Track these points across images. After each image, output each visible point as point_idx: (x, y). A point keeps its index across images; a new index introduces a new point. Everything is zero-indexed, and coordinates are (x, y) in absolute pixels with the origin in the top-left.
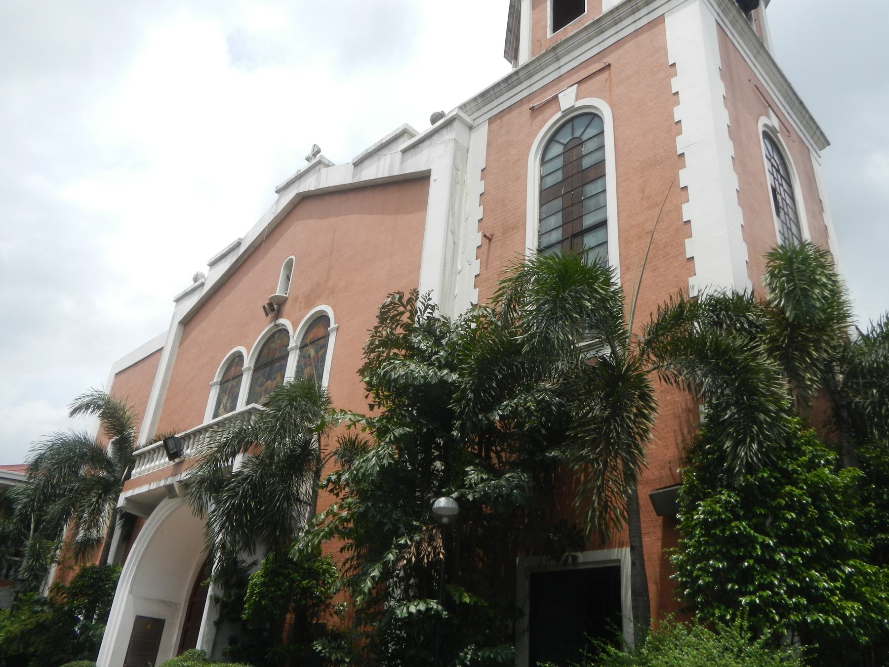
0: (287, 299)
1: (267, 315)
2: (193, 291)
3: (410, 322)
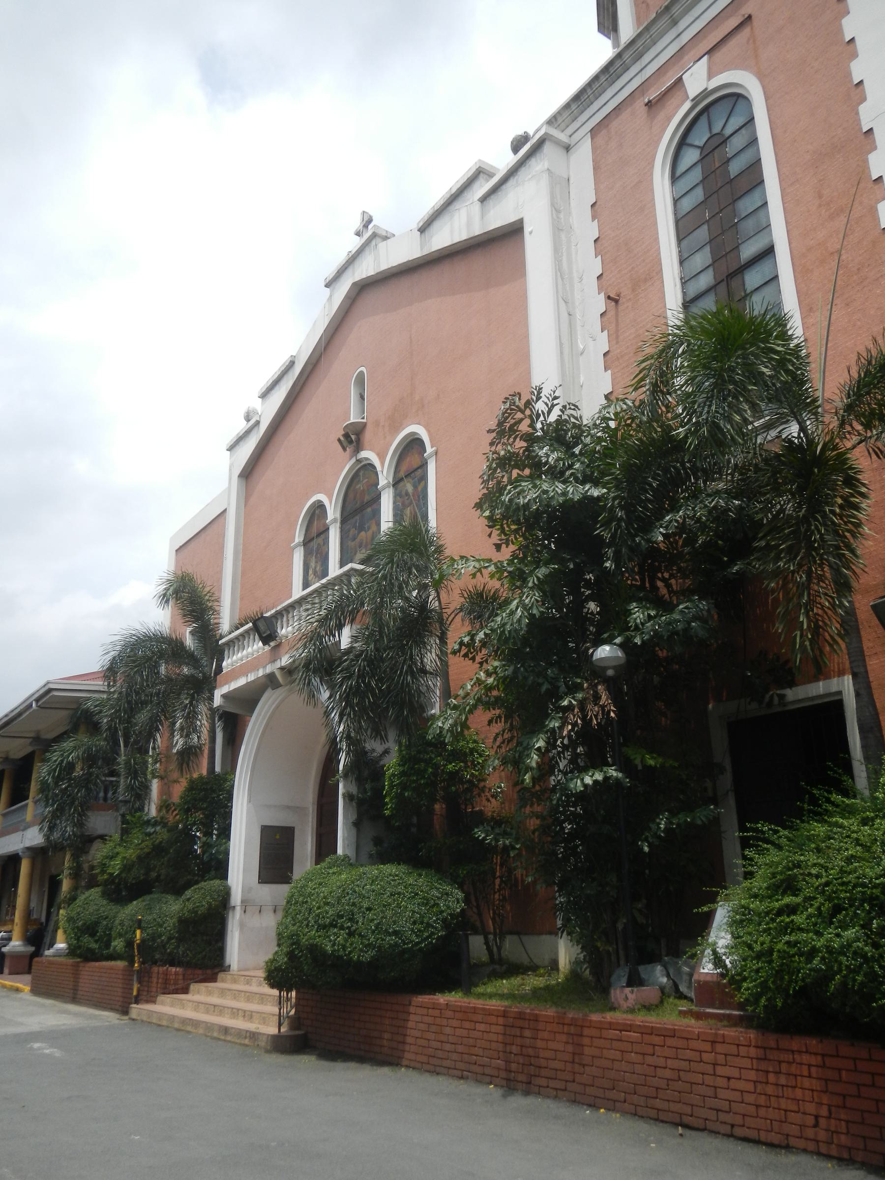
0: (364, 425)
1: (344, 449)
2: (247, 433)
3: (530, 430)
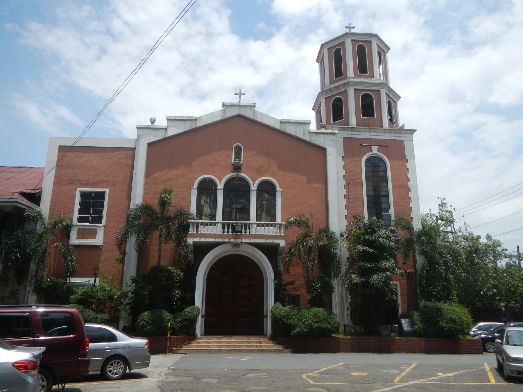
0: (242, 165)
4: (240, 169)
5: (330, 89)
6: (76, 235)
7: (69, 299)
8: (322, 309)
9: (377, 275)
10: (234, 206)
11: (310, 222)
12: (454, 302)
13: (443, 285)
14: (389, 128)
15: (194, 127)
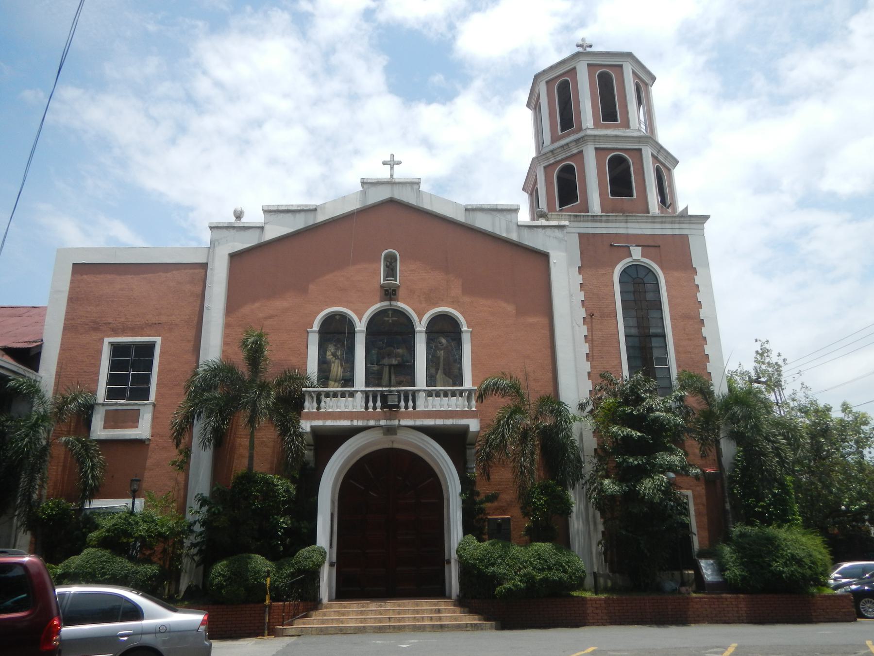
0: (398, 287)
4: (395, 294)
5: (552, 151)
6: (103, 423)
7: (87, 540)
8: (550, 544)
9: (651, 479)
10: (386, 361)
11: (523, 384)
12: (796, 525)
13: (774, 495)
14: (660, 215)
15: (311, 223)
